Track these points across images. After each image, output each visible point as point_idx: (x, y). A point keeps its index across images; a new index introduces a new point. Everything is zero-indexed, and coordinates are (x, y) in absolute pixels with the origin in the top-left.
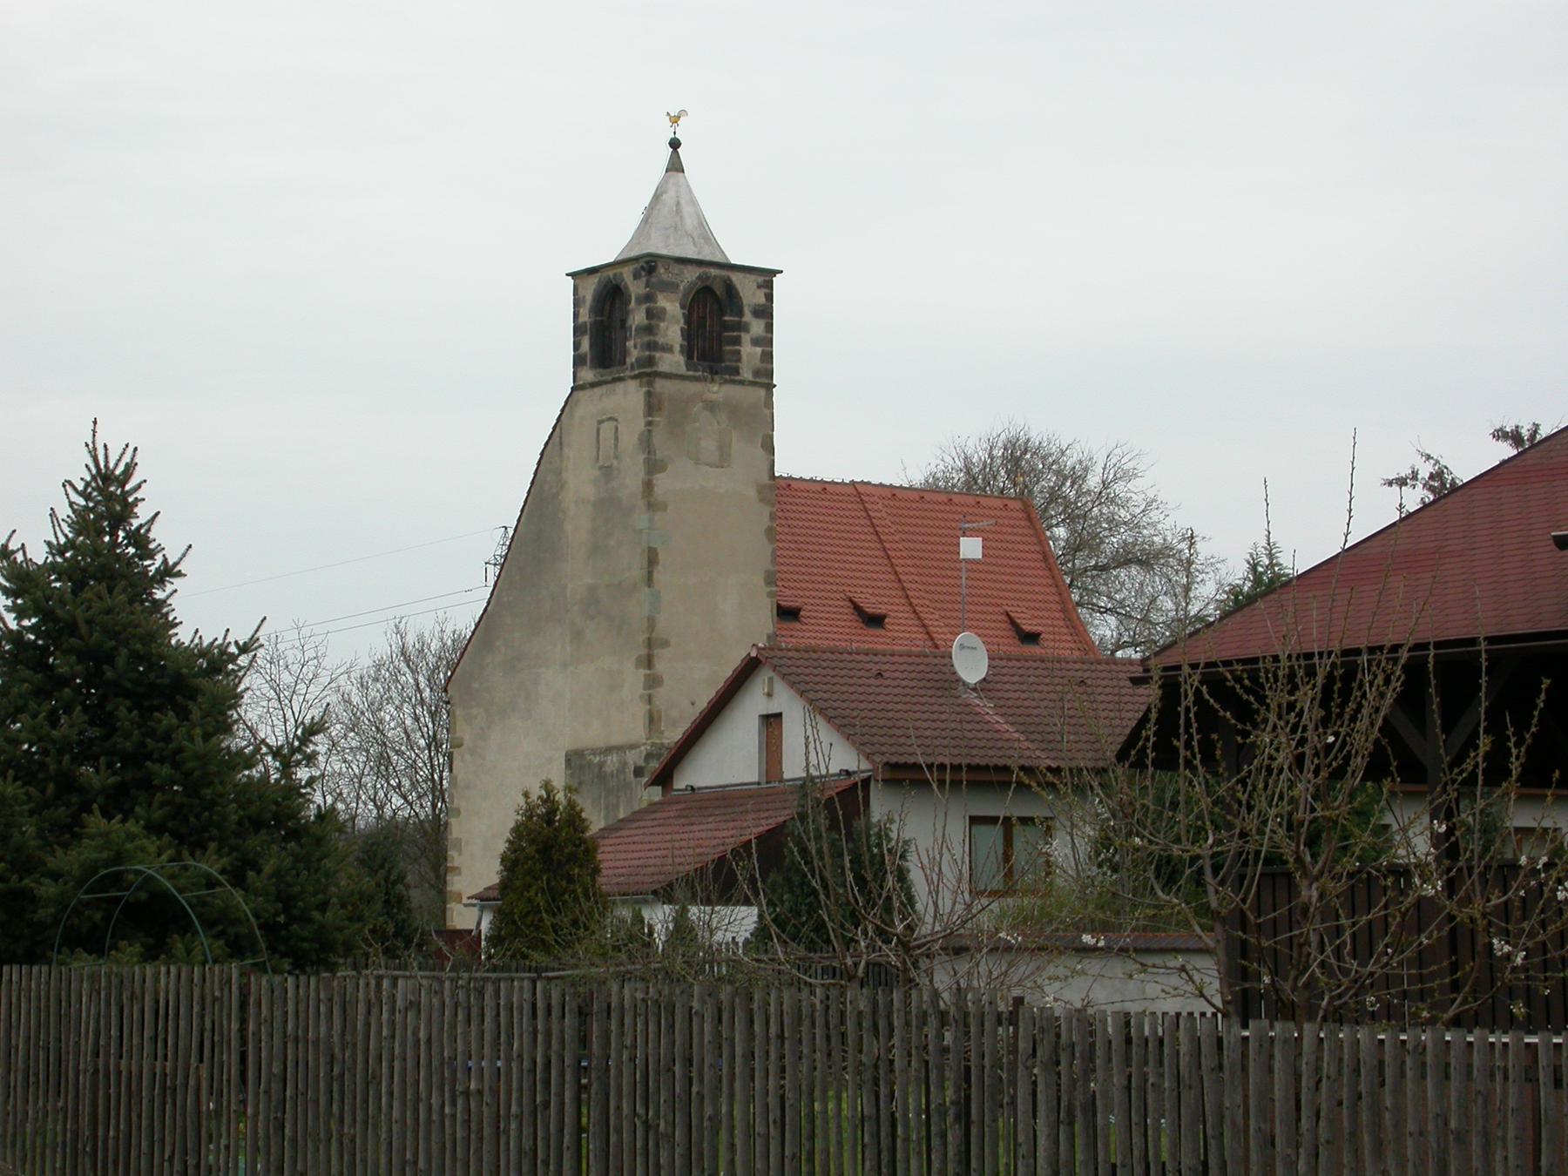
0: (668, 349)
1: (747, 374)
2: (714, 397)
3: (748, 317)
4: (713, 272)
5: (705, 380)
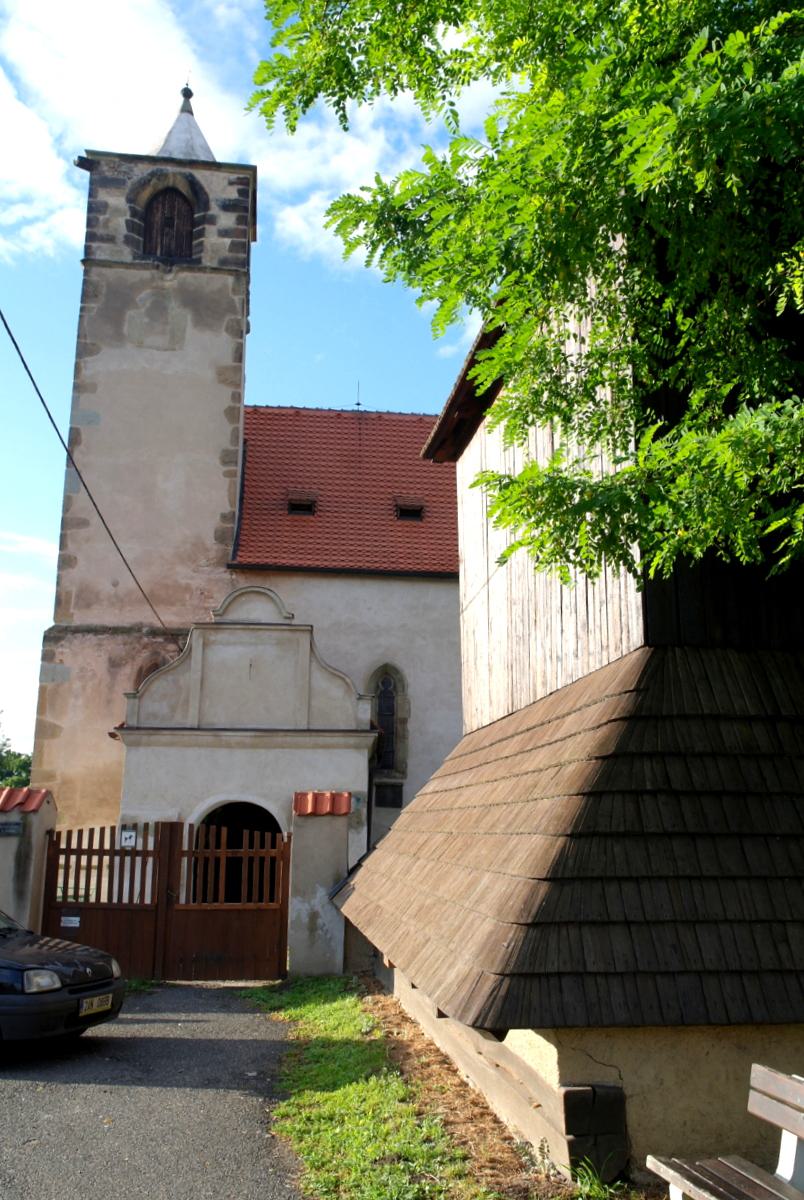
1: (208, 260)
3: (214, 210)
4: (170, 169)
5: (157, 267)
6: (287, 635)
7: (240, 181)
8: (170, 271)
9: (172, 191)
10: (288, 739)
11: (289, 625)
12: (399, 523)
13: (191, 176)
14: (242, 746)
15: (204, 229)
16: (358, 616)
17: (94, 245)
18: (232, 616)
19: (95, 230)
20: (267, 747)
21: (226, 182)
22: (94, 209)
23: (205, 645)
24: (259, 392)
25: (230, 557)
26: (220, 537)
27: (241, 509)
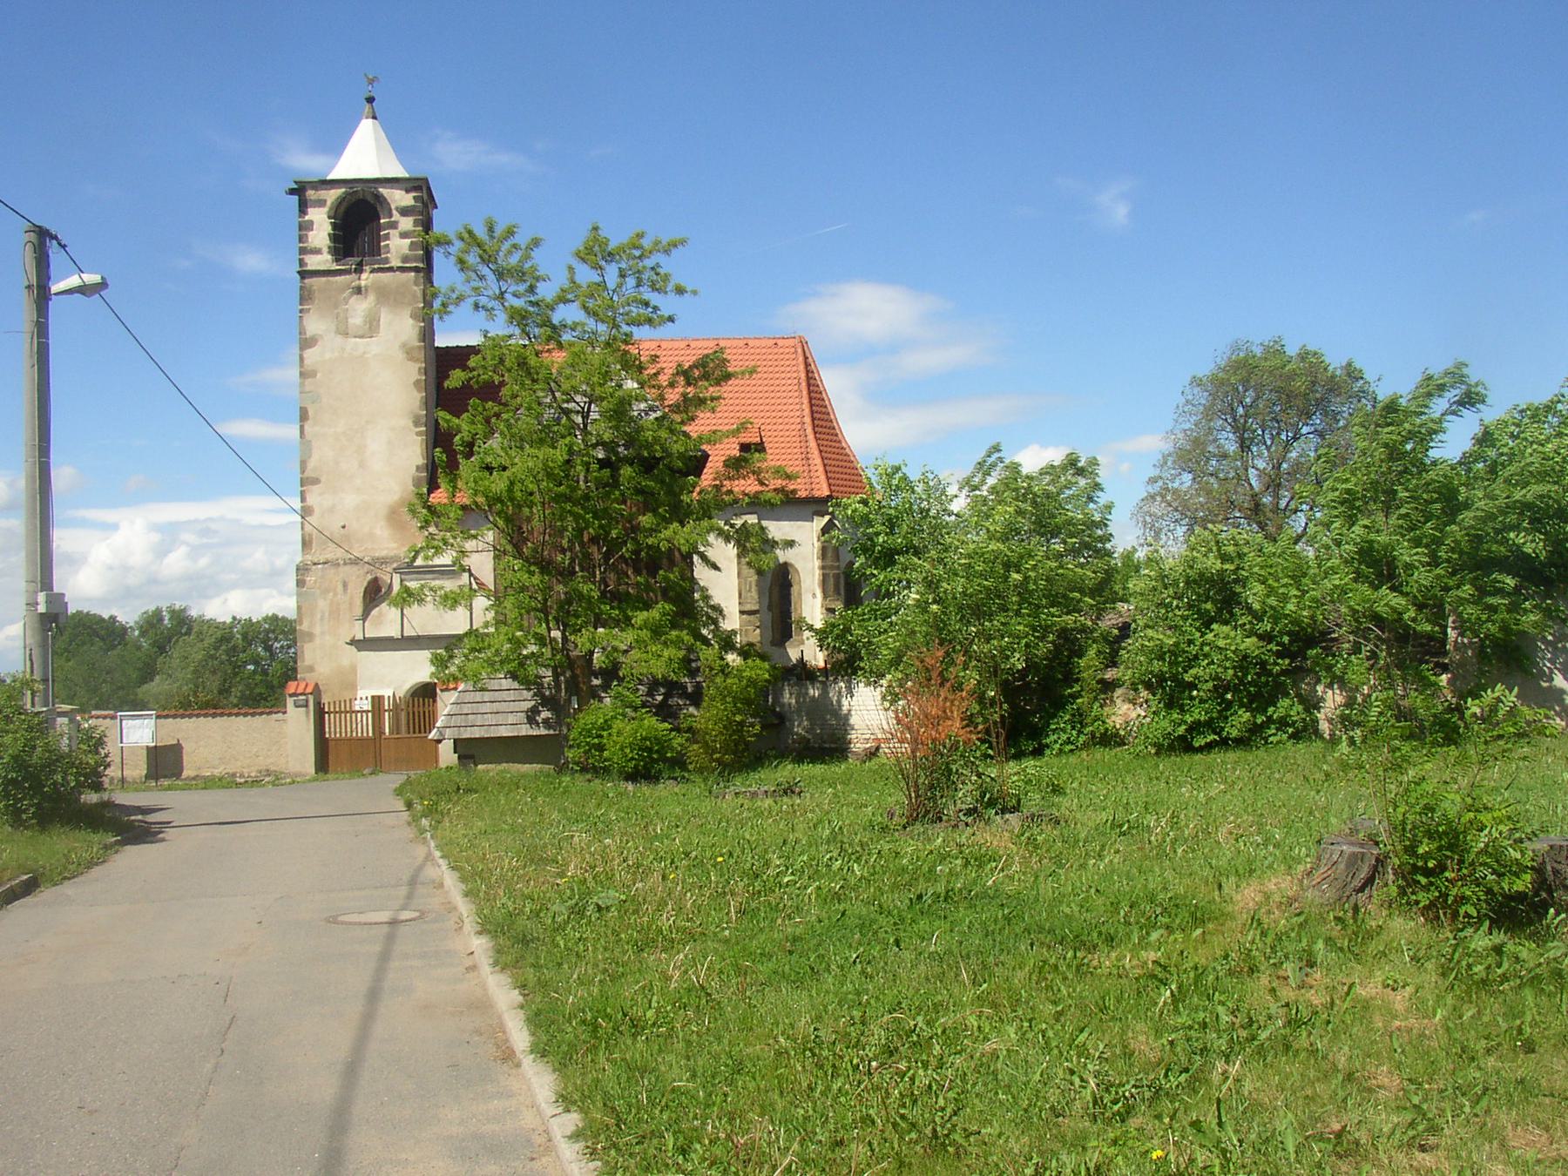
0: (317, 251)
3: (396, 216)
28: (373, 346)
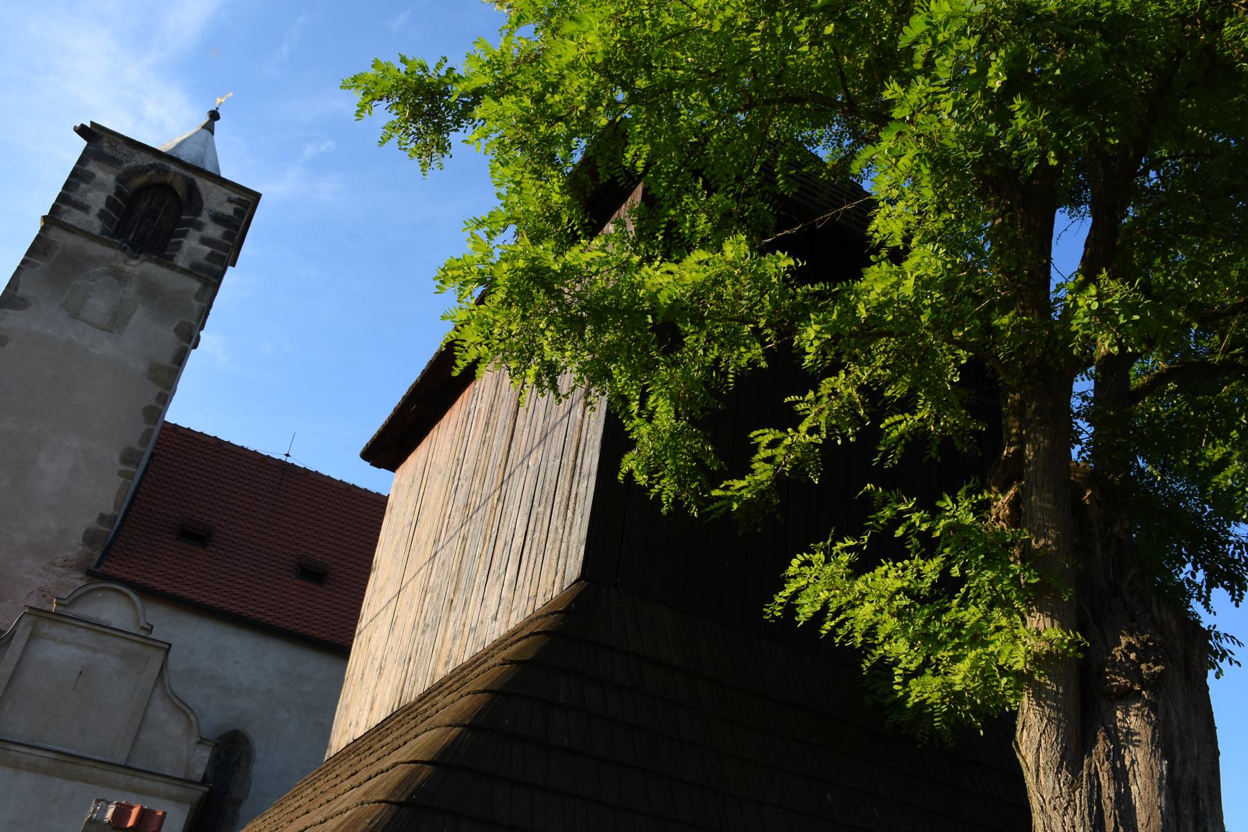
0: (85, 208)
1: (182, 260)
2: (128, 268)
3: (204, 218)
4: (173, 167)
5: (124, 249)
6: (137, 647)
7: (239, 202)
8: (136, 258)
9: (168, 188)
10: (96, 772)
11: (145, 637)
12: (297, 581)
13: (193, 182)
14: (34, 768)
15: (187, 231)
16: (228, 665)
17: (64, 207)
18: (77, 611)
19: (71, 194)
20: (70, 777)
21: (225, 198)
22: (78, 176)
23: (32, 636)
24: (185, 411)
25: (93, 565)
26: (90, 538)
27: (123, 519)
28: (105, 346)
